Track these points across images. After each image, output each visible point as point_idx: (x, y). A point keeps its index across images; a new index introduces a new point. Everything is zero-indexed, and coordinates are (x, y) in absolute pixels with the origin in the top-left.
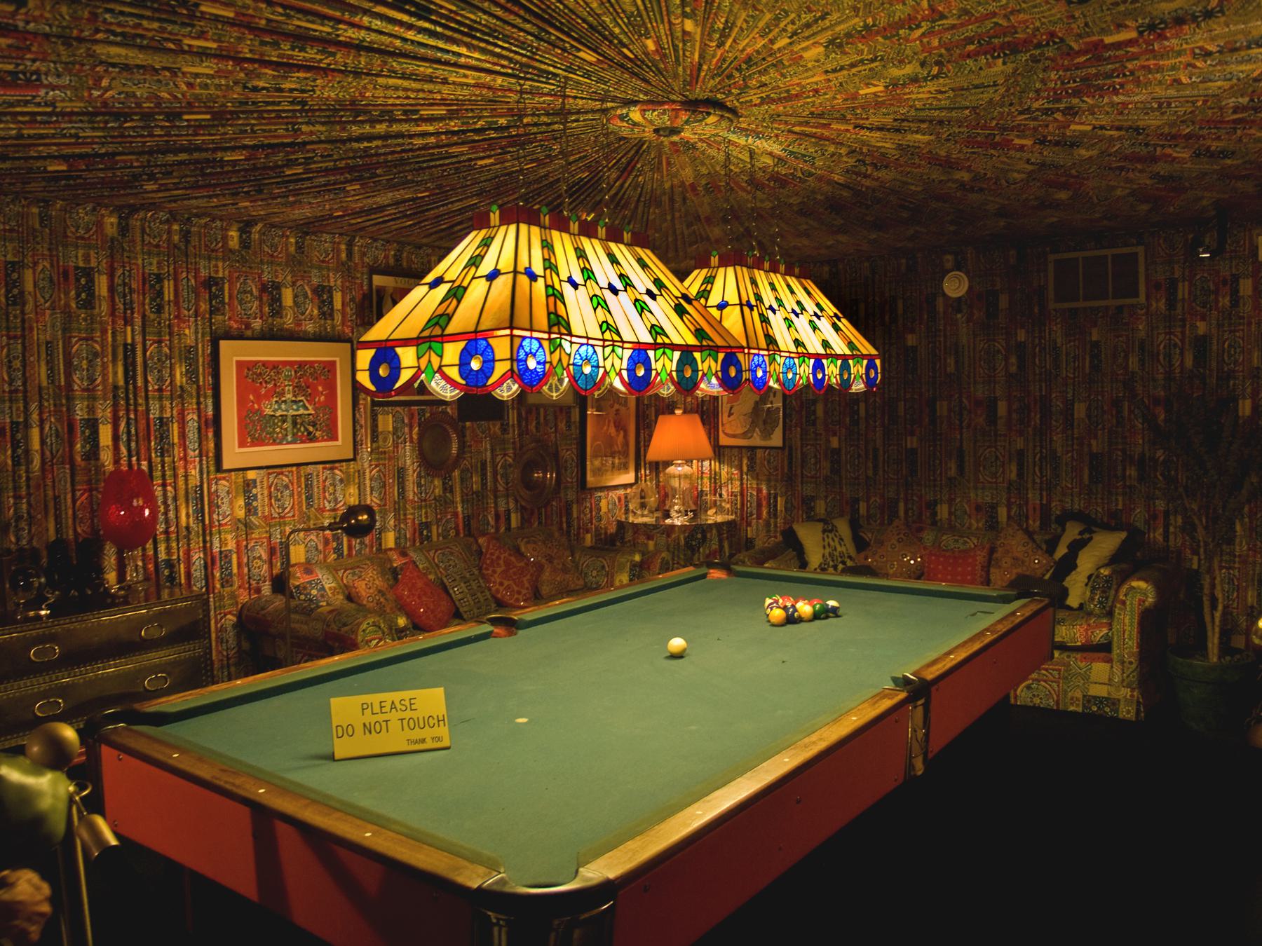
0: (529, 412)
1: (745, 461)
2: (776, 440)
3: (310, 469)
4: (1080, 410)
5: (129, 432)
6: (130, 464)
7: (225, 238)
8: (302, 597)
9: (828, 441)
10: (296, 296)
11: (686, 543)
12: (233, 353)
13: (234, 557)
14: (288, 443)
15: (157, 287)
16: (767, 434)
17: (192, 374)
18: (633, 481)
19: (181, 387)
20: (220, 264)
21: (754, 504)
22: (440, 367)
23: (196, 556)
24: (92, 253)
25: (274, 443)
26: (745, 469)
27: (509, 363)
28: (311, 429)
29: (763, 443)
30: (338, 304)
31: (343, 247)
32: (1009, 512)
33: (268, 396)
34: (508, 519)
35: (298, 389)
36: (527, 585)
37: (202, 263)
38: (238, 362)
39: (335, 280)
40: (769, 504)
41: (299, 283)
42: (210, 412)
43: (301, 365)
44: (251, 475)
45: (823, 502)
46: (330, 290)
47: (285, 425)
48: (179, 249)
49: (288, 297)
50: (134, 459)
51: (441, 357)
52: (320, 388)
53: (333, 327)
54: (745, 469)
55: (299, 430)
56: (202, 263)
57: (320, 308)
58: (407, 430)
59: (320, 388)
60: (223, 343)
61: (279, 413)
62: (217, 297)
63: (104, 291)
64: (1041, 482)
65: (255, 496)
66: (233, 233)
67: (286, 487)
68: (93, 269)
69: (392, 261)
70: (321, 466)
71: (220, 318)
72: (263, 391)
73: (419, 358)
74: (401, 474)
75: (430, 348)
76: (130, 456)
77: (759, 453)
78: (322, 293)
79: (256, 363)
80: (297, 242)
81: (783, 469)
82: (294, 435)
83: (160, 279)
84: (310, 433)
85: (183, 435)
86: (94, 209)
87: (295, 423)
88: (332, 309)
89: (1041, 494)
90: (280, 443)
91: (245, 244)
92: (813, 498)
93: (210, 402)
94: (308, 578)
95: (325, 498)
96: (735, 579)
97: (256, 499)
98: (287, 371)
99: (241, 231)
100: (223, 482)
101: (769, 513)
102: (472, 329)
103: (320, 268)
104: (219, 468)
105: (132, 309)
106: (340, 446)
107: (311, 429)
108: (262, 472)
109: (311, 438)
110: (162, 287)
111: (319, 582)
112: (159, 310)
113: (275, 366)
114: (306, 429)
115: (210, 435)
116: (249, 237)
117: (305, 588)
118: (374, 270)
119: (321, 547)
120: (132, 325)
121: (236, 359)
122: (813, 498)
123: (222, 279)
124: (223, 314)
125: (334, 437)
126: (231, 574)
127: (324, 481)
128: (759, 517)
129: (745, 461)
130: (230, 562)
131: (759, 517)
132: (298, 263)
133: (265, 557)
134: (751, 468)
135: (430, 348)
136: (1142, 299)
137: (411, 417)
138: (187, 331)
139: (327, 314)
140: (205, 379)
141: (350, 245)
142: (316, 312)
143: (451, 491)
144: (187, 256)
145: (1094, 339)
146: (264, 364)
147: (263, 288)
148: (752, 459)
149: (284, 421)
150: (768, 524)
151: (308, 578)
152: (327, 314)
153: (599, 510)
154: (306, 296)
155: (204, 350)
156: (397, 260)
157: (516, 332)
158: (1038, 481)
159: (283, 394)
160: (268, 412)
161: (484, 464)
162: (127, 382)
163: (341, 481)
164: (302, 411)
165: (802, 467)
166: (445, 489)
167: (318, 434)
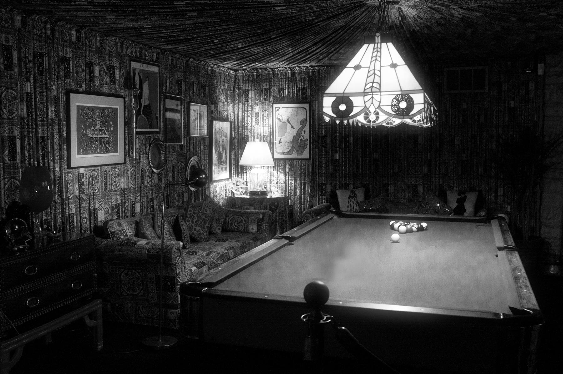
0: (190, 140)
1: (287, 166)
2: (306, 154)
3: (105, 168)
4: (457, 141)
5: (29, 144)
6: (30, 164)
7: (70, 35)
8: (115, 238)
9: (333, 156)
10: (100, 71)
11: (270, 207)
12: (78, 101)
13: (75, 217)
14: (98, 153)
15: (40, 60)
16: (300, 152)
17: (57, 112)
18: (228, 177)
19: (52, 119)
20: (68, 50)
21: (293, 188)
22: (379, 106)
23: (58, 217)
24: (10, 36)
25: (92, 153)
26: (287, 170)
27: (423, 105)
28: (107, 145)
29: (300, 157)
30: (117, 77)
31: (119, 45)
32: (424, 188)
33: (90, 126)
34: (183, 196)
35: (103, 123)
36: (206, 230)
37: (60, 48)
38: (78, 106)
39: (116, 64)
40: (301, 188)
41: (101, 63)
42: (65, 135)
43: (104, 109)
44: (82, 171)
45: (329, 186)
46: (114, 69)
47: (97, 143)
48: (50, 39)
49: (96, 69)
50: (32, 160)
51: (380, 102)
52: (111, 123)
53: (115, 89)
54: (287, 170)
55: (102, 146)
56: (60, 48)
57: (110, 78)
58: (144, 147)
59: (111, 123)
60: (72, 95)
61: (94, 136)
62: (67, 68)
63: (15, 61)
64: (439, 174)
65: (83, 183)
66: (74, 32)
67: (96, 178)
68: (11, 46)
69: (138, 54)
70: (110, 167)
71: (68, 80)
72: (88, 123)
73: (365, 102)
74: (143, 169)
75: (372, 97)
76: (30, 159)
77: (295, 162)
78: (111, 69)
79: (86, 106)
80: (100, 40)
81: (308, 168)
82: (100, 148)
83: (41, 56)
84: (107, 148)
85: (53, 147)
86: (11, 10)
87: (101, 142)
88: (115, 79)
89: (439, 180)
90: (94, 153)
91: (78, 39)
92: (325, 184)
93: (65, 128)
94: (119, 228)
95: (112, 184)
96: (343, 220)
97: (84, 185)
98: (98, 113)
99: (78, 31)
100: (70, 174)
101: (301, 192)
102: (342, 92)
103: (110, 55)
104: (69, 167)
105: (30, 72)
106: (116, 157)
107: (107, 145)
108: (86, 169)
109: (107, 151)
110: (43, 61)
111: (124, 231)
112: (41, 73)
113: (93, 109)
114: (105, 146)
115: (65, 147)
116: (80, 35)
117: (117, 234)
118: (133, 59)
119: (110, 212)
120: (30, 82)
121: (77, 104)
122: (325, 184)
123: (69, 58)
124: (70, 78)
125: (116, 151)
126: (74, 227)
127: (112, 175)
128: (295, 194)
129: (287, 166)
130: (73, 220)
131: (295, 194)
132: (100, 51)
133: (87, 218)
134: (290, 169)
135: (372, 97)
136: (487, 89)
137: (146, 140)
138: (54, 87)
139: (113, 81)
140: (63, 116)
141: (122, 44)
142: (108, 80)
143: (161, 181)
144: (53, 43)
145: (465, 107)
146: (89, 108)
147: (86, 65)
148: (291, 166)
149: (96, 141)
150: (300, 198)
151: (119, 228)
152: (113, 81)
153: (216, 192)
154: (104, 71)
155: (62, 99)
156: (140, 54)
157: (382, 93)
158: (437, 173)
159: (95, 126)
160: (90, 135)
161: (173, 167)
162: (28, 115)
163: (119, 175)
164: (103, 136)
165: (319, 169)
166: (159, 180)
167: (110, 148)
